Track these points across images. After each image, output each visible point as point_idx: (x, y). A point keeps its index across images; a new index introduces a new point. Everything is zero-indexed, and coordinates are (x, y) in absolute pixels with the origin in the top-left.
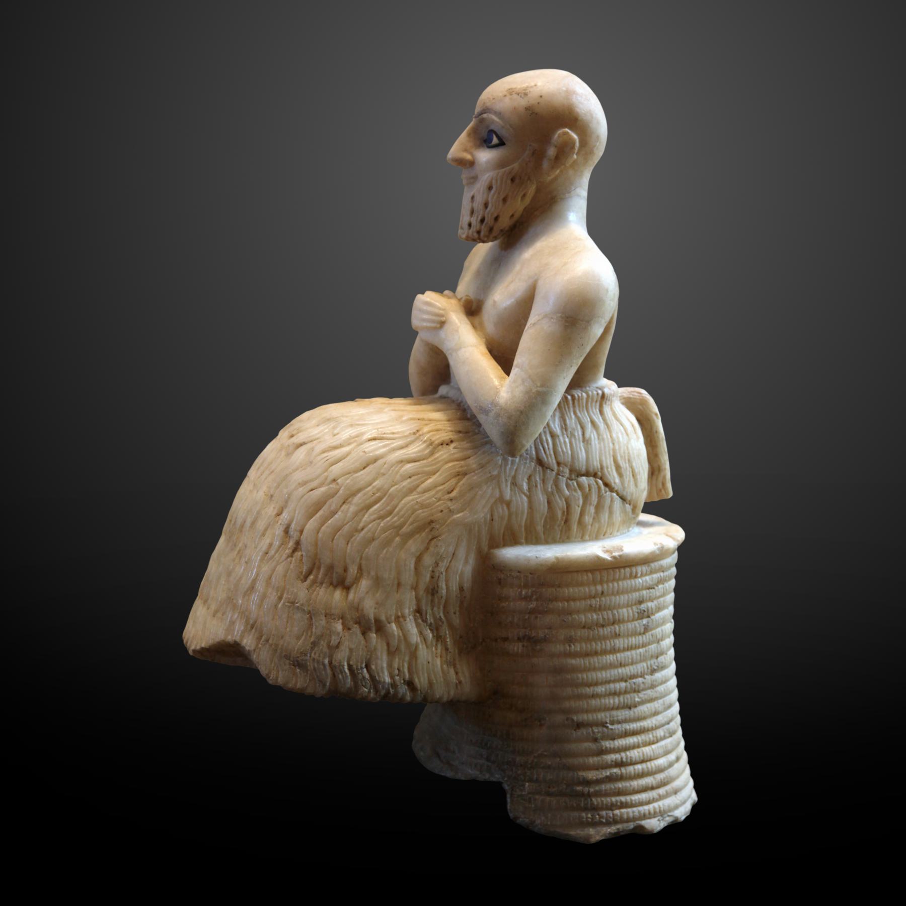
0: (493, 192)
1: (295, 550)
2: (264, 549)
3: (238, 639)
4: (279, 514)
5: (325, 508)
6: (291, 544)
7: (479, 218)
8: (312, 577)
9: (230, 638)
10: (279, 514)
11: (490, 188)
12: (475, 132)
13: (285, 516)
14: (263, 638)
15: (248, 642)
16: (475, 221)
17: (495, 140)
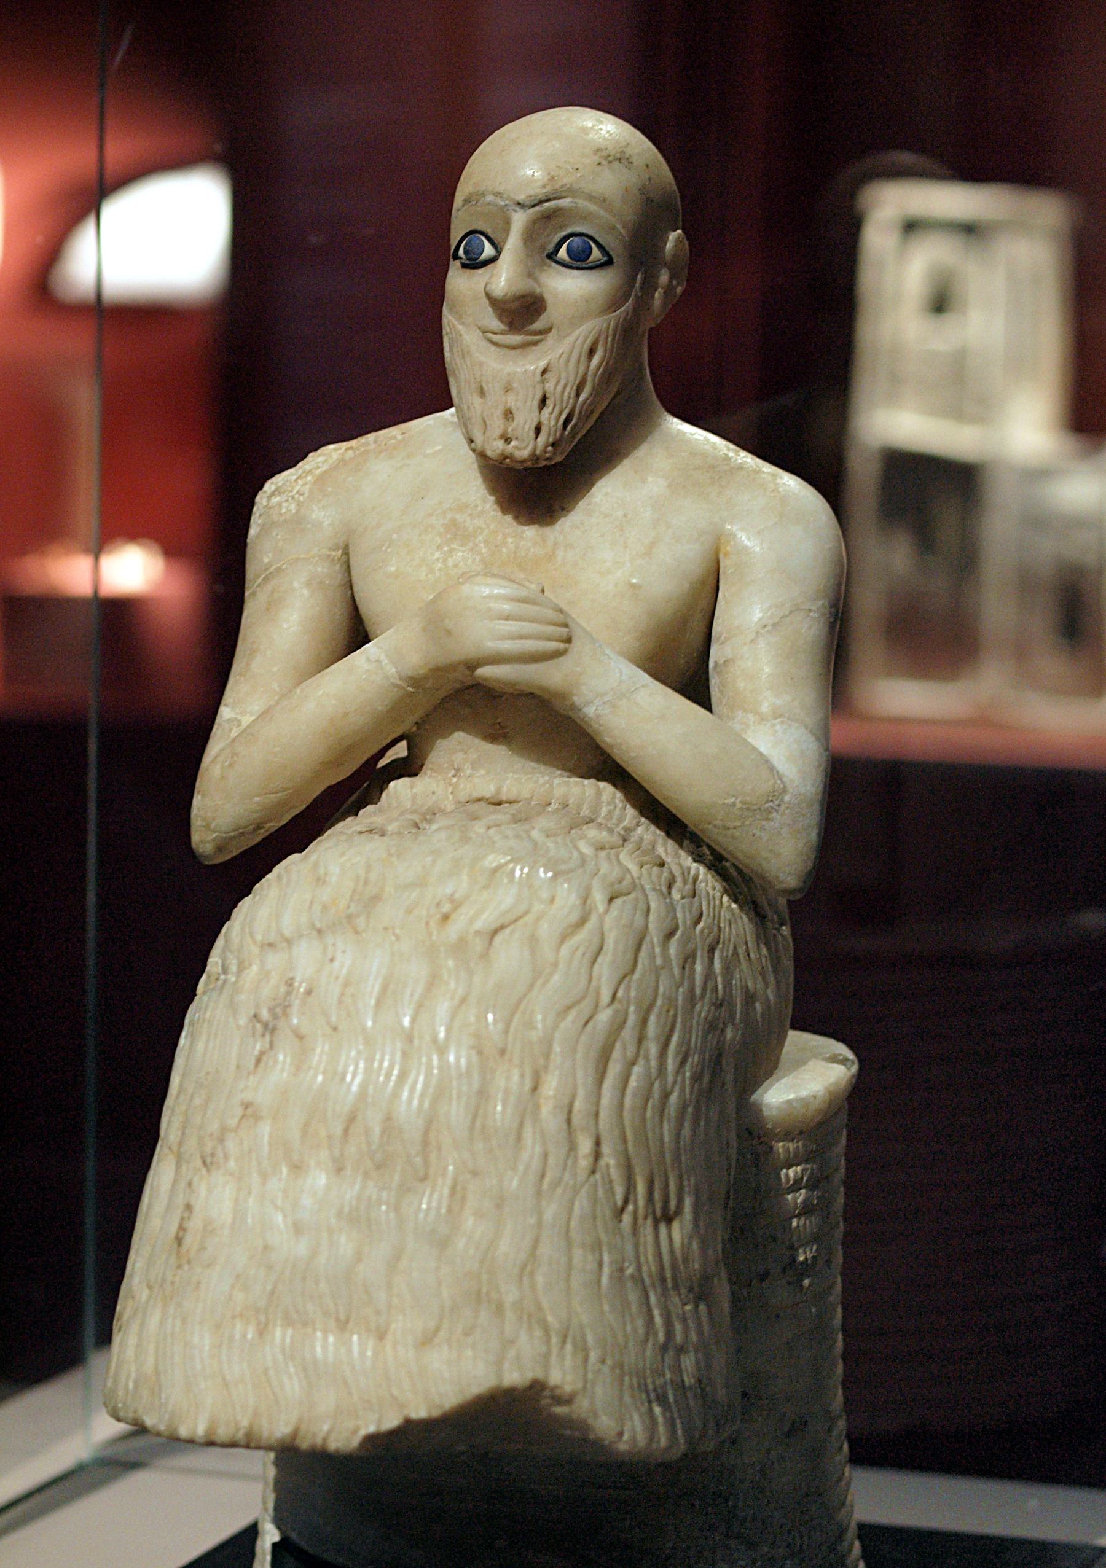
0: (596, 360)
1: (597, 1155)
2: (536, 1164)
3: (539, 1374)
4: (535, 1089)
5: (616, 1054)
6: (585, 1146)
7: (563, 417)
8: (631, 1207)
9: (514, 1377)
10: (535, 1089)
11: (592, 352)
12: (530, 236)
13: (551, 1085)
14: (593, 1356)
15: (561, 1375)
16: (550, 418)
17: (596, 253)
